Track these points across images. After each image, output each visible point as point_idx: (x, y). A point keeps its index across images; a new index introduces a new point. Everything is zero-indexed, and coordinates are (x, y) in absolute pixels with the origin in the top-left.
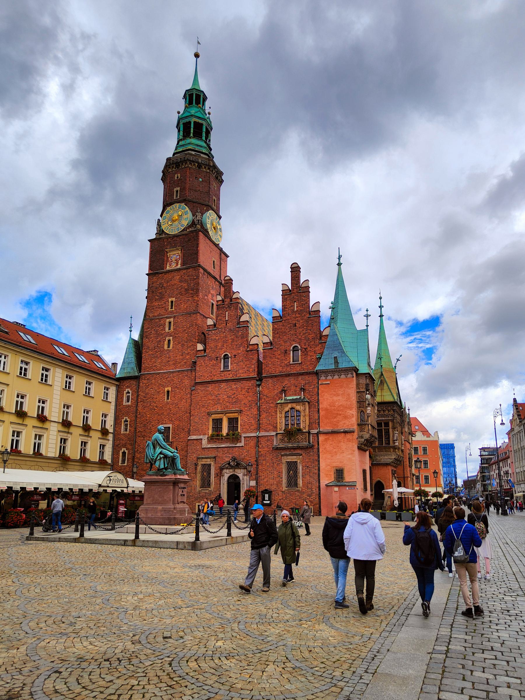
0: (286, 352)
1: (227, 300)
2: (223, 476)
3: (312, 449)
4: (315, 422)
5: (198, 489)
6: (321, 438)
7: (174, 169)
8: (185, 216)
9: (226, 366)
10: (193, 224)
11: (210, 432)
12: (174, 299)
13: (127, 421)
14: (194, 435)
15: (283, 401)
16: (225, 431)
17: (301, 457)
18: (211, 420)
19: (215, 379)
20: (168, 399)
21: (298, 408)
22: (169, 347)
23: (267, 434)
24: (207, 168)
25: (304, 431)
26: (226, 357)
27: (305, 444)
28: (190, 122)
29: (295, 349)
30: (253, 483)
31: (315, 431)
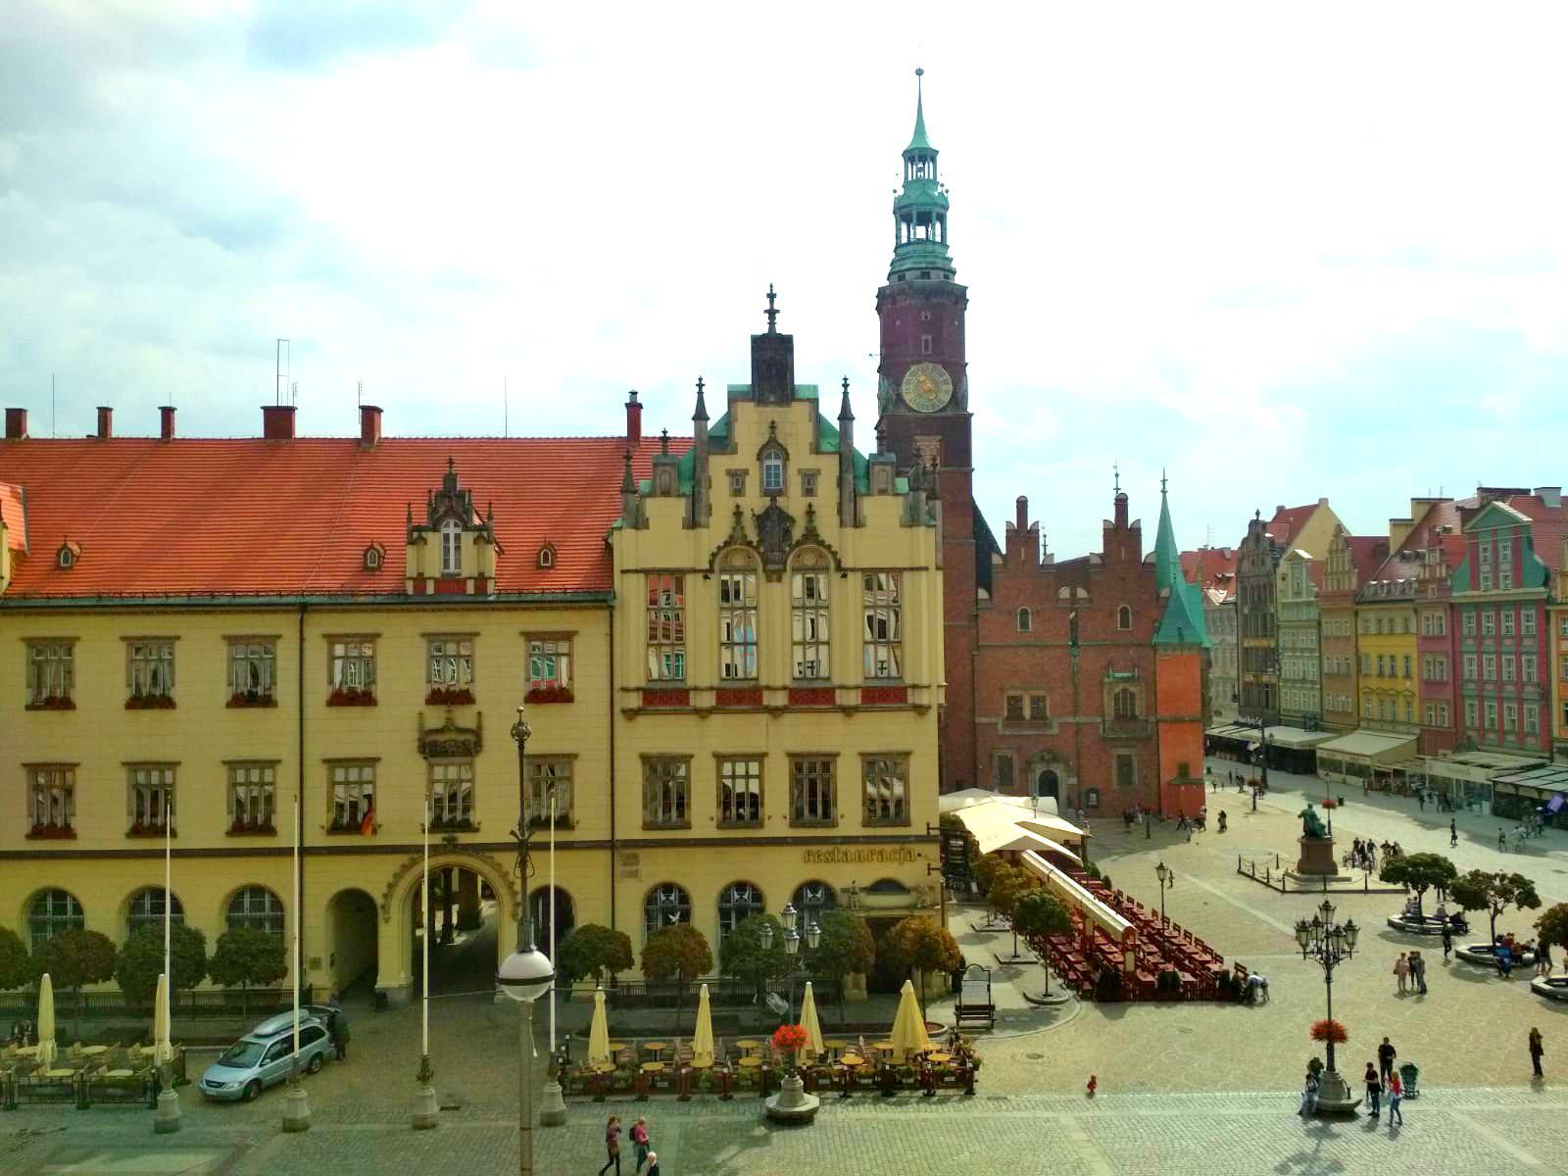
0: (1111, 614)
2: (1034, 771)
3: (1149, 742)
4: (1152, 708)
6: (1161, 725)
8: (944, 387)
9: (1024, 625)
11: (1006, 713)
14: (982, 716)
15: (1111, 679)
16: (1027, 713)
18: (1005, 699)
21: (1132, 689)
26: (1024, 613)
27: (1144, 734)
29: (1124, 611)
30: (1073, 781)
31: (1153, 719)
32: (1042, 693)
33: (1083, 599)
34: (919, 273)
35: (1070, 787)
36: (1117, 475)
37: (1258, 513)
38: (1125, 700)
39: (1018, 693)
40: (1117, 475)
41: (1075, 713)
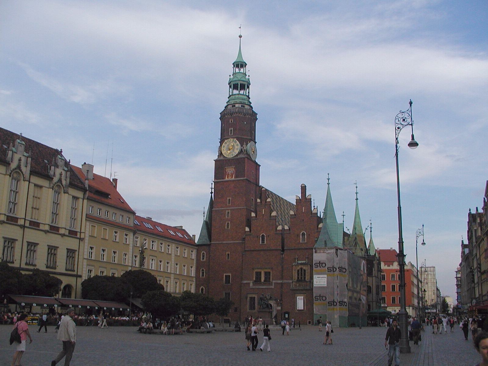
0: (298, 236)
1: (263, 202)
5: (248, 310)
7: (229, 116)
10: (241, 152)
11: (254, 279)
12: (230, 198)
13: (204, 270)
16: (263, 279)
17: (306, 295)
19: (257, 249)
20: (228, 258)
21: (304, 268)
22: (228, 227)
23: (288, 281)
24: (249, 115)
25: (308, 280)
28: (238, 84)
29: (303, 234)
30: (279, 308)
32: (269, 270)
33: (287, 230)
34: (231, 106)
35: (278, 310)
36: (357, 187)
37: (470, 210)
38: (301, 273)
39: (259, 270)
40: (357, 187)
41: (282, 278)
